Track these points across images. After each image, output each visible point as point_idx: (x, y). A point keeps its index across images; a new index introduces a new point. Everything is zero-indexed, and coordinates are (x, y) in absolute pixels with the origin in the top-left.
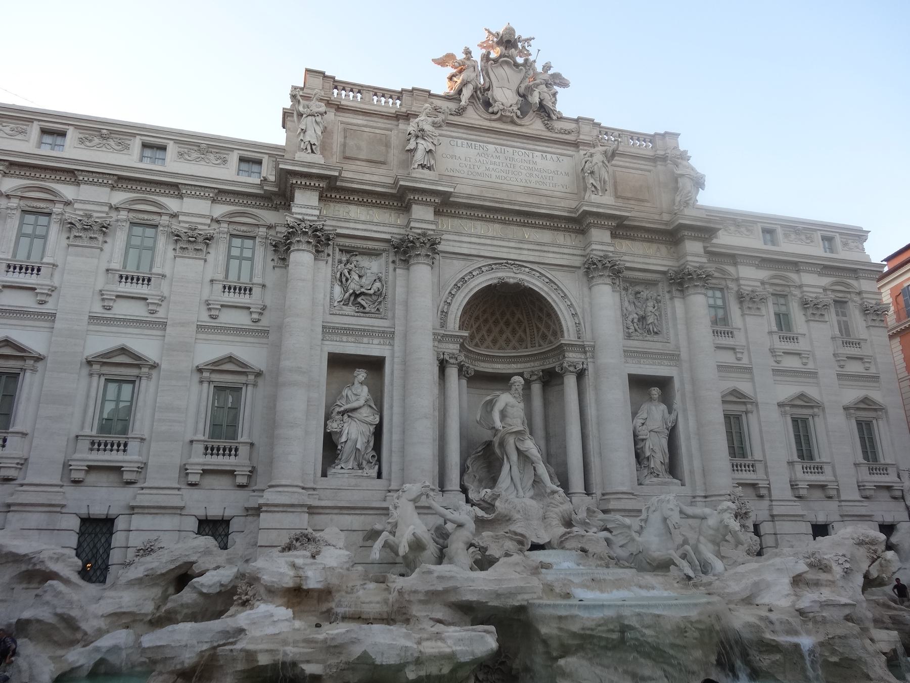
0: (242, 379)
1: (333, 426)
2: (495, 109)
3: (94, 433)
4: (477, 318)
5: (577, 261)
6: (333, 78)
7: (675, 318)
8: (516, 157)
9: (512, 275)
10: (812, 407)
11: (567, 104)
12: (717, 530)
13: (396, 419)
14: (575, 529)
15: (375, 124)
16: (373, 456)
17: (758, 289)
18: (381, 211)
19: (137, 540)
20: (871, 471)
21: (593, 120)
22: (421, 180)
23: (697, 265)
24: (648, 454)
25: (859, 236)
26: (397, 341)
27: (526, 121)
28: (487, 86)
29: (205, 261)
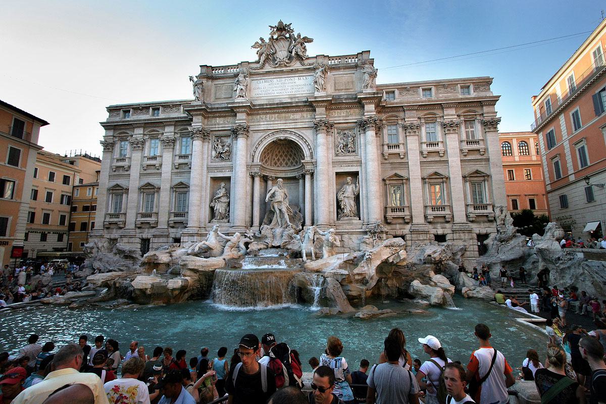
0: (186, 190)
1: (212, 204)
2: (276, 62)
4: (276, 155)
6: (211, 66)
9: (283, 135)
13: (233, 201)
17: (414, 122)
19: (155, 246)
20: (475, 208)
23: (369, 116)
24: (342, 207)
25: (487, 82)
27: (292, 64)
28: (274, 51)
29: (173, 149)
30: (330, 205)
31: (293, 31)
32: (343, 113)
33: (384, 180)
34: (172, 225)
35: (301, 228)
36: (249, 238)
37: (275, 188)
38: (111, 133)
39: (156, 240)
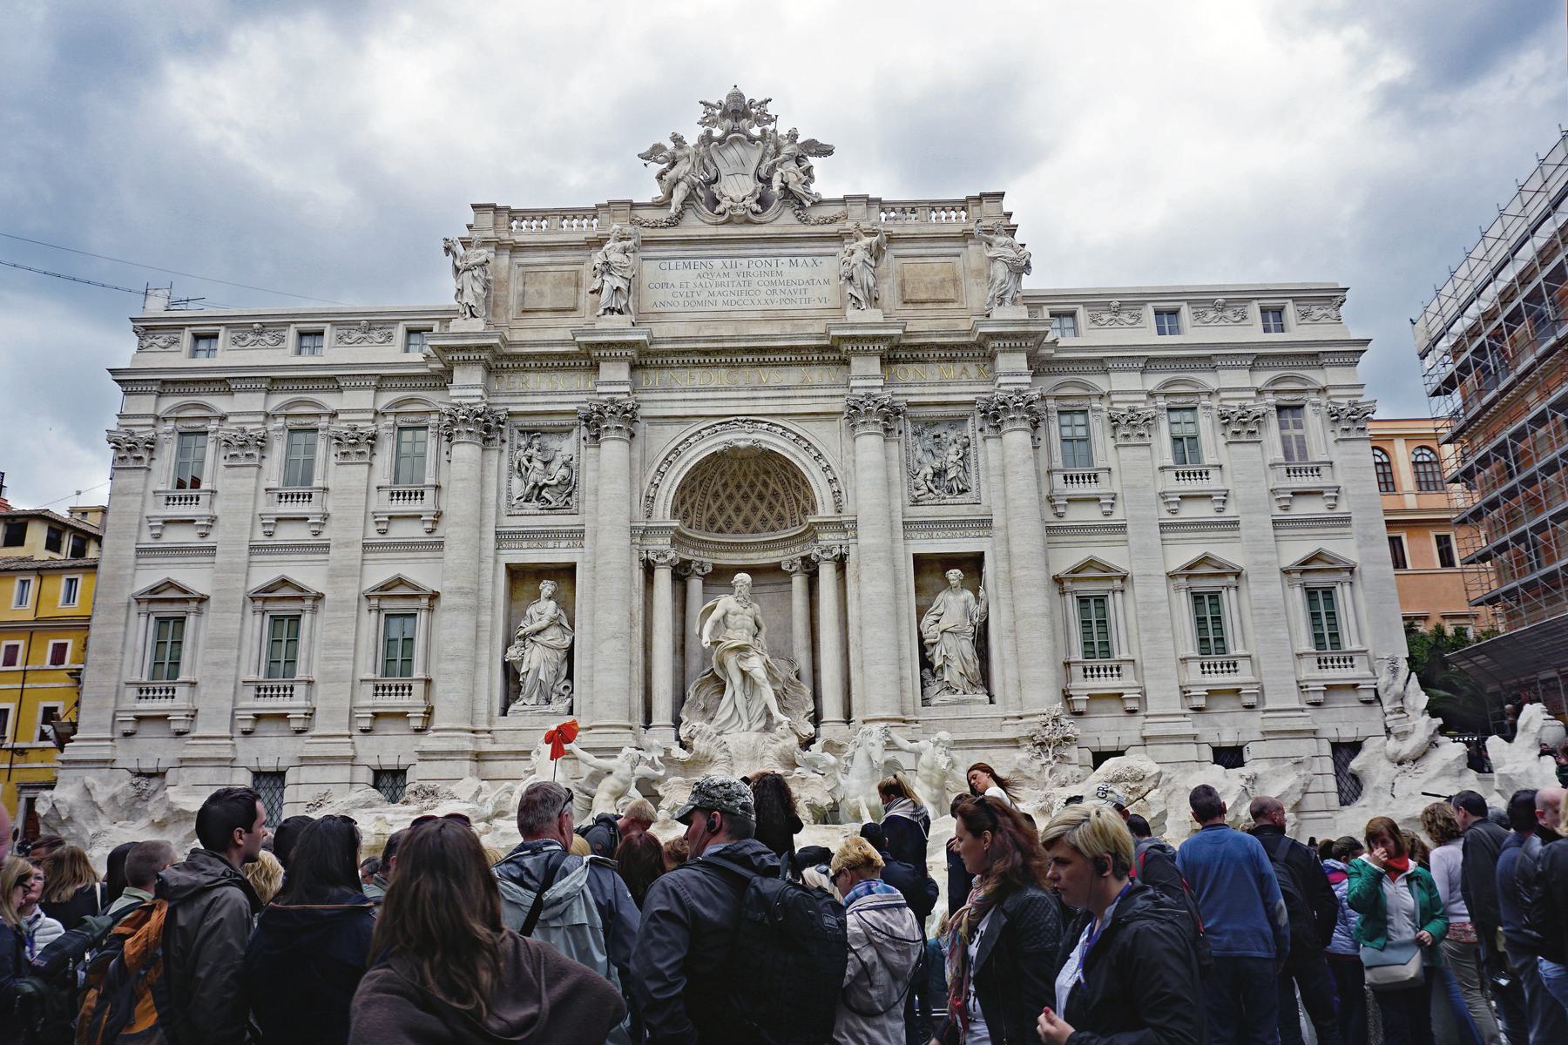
1: (513, 653)
3: (261, 678)
4: (716, 495)
5: (838, 405)
6: (508, 208)
7: (987, 469)
8: (753, 269)
9: (744, 436)
10: (1224, 575)
11: (828, 181)
12: (932, 768)
14: (798, 770)
15: (562, 260)
16: (566, 688)
18: (567, 375)
21: (866, 197)
22: (603, 332)
23: (1012, 388)
24: (938, 662)
26: (587, 542)
28: (713, 175)
29: (371, 465)
30: (900, 660)
31: (771, 120)
32: (934, 372)
33: (1058, 580)
34: (366, 724)
35: (812, 730)
36: (651, 763)
37: (726, 602)
38: (146, 404)
39: (308, 774)
